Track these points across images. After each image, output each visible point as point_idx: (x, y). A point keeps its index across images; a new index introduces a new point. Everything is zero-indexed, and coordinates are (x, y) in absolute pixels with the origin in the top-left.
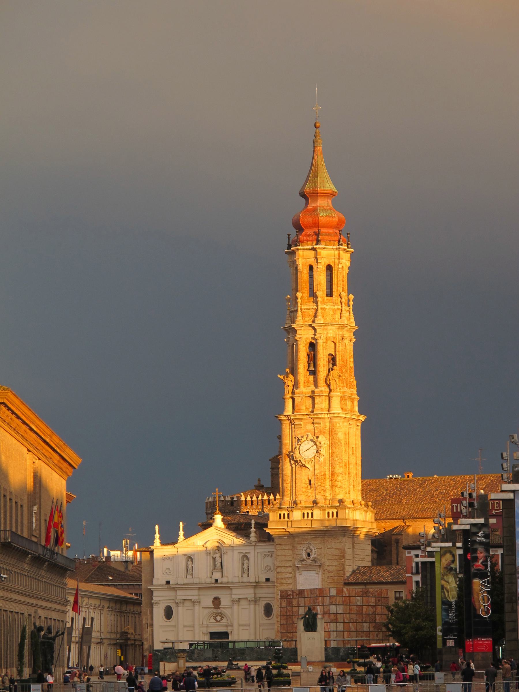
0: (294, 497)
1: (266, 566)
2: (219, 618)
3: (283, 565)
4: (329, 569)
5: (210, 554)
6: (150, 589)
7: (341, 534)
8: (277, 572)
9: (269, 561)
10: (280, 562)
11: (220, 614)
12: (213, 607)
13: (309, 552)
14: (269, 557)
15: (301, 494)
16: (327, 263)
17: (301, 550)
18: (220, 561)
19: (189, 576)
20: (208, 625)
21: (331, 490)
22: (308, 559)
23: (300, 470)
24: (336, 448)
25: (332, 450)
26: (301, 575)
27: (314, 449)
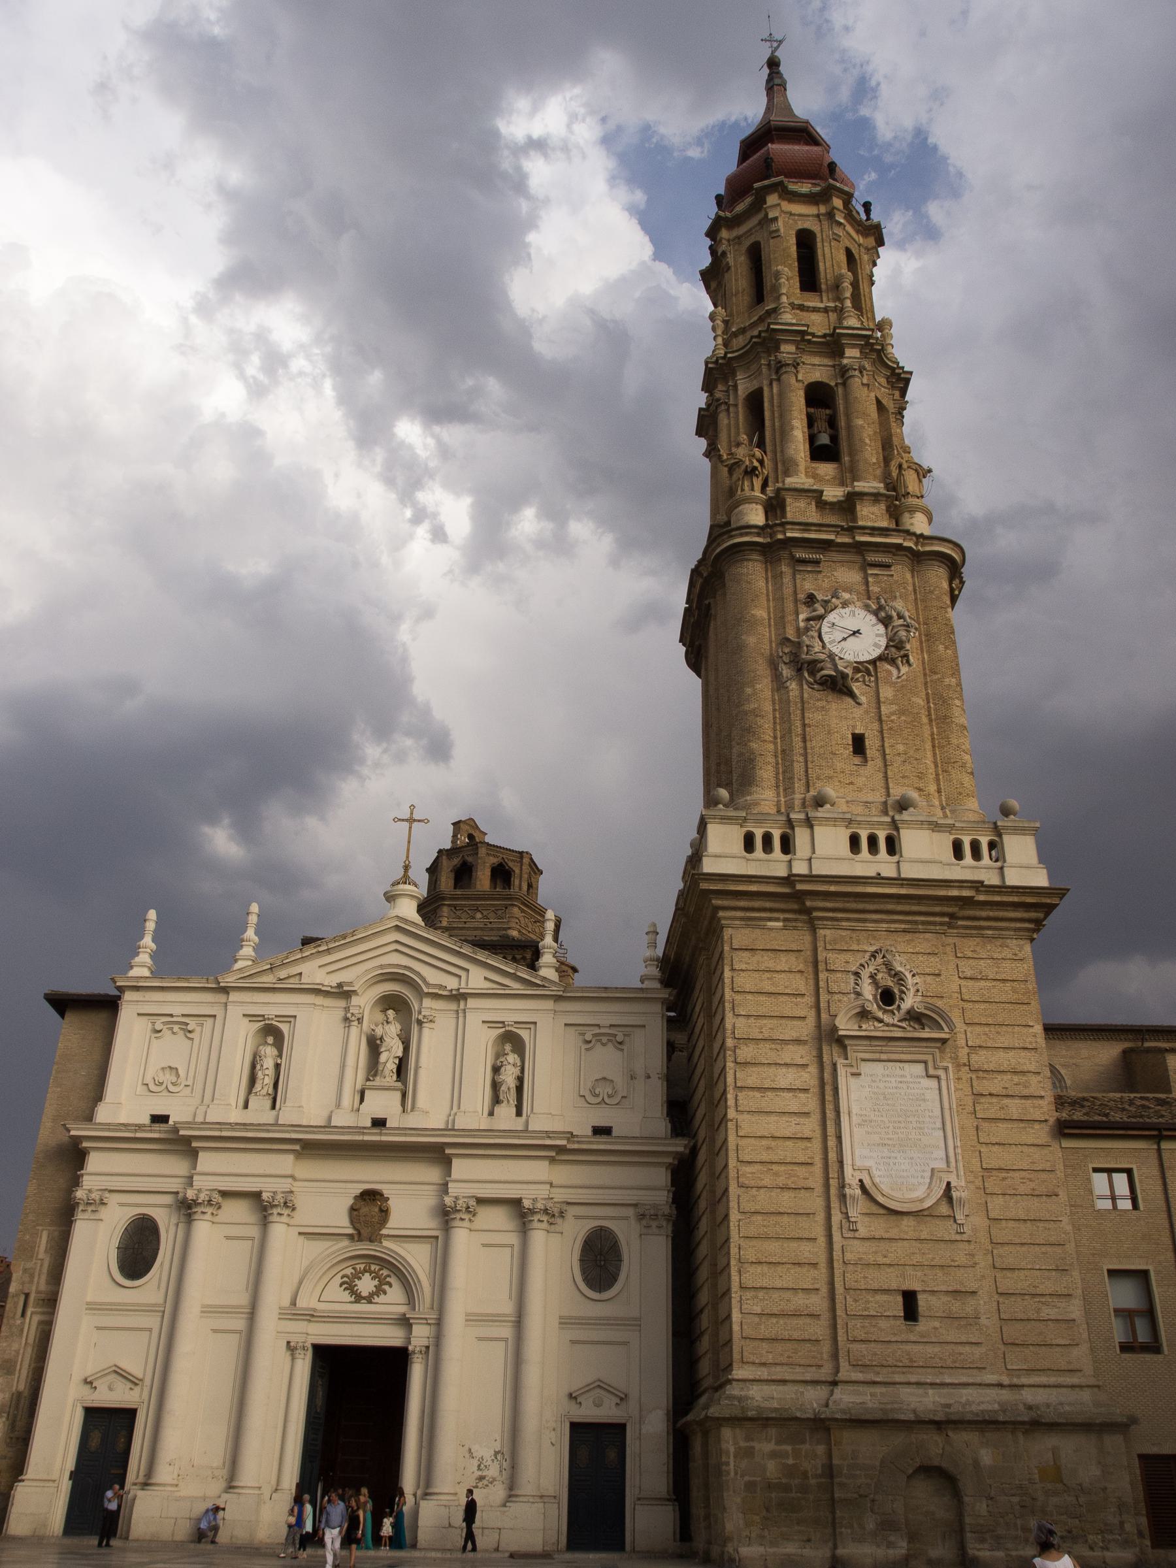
0: (799, 786)
1: (597, 1080)
2: (366, 1285)
3: (767, 1036)
4: (979, 1059)
5: (360, 1021)
6: (77, 1140)
7: (1019, 925)
8: (738, 1060)
9: (607, 1060)
10: (752, 1020)
11: (373, 1267)
12: (350, 1231)
13: (890, 984)
14: (610, 1045)
15: (831, 778)
16: (848, 244)
17: (852, 977)
18: (400, 1054)
19: (260, 1103)
20: (315, 1310)
21: (941, 777)
22: (885, 1011)
23: (820, 700)
24: (946, 648)
25: (929, 652)
26: (853, 1081)
27: (877, 635)
